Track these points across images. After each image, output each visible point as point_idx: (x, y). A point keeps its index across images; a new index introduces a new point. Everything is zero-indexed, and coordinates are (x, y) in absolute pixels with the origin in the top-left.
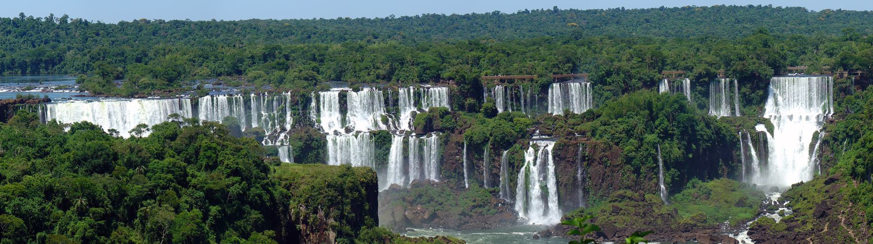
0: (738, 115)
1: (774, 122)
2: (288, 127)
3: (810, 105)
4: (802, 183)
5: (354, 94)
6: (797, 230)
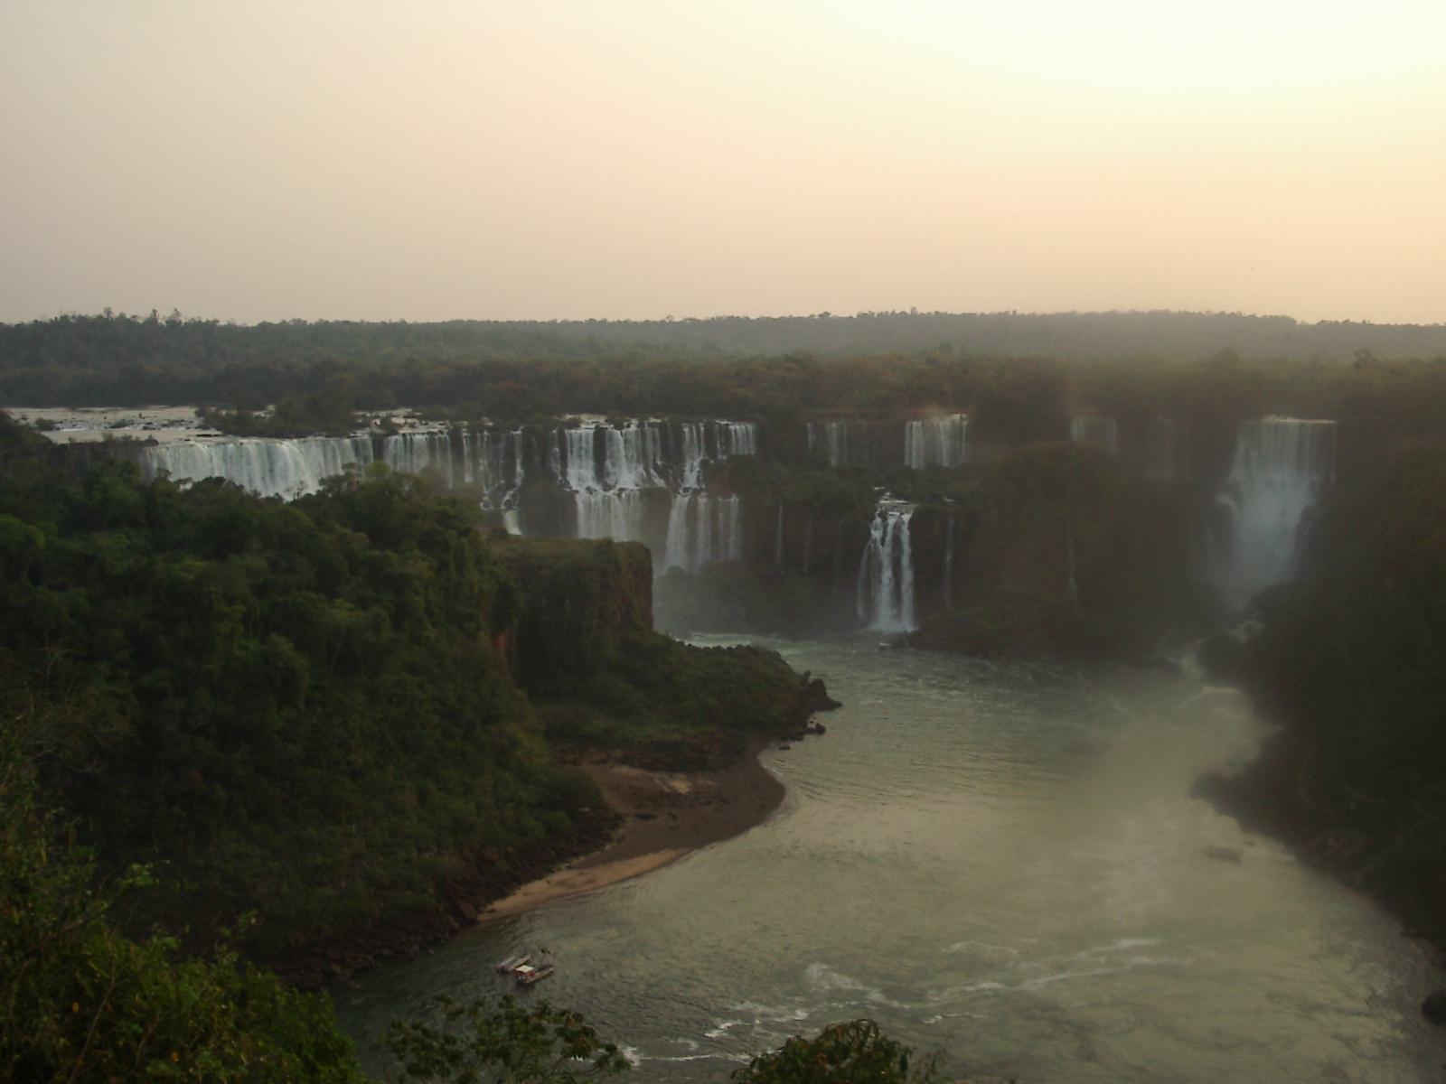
2: (518, 481)
5: (619, 432)
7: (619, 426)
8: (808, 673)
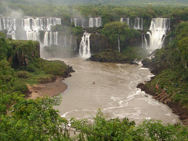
2: (15, 29)
3: (163, 27)
5: (34, 20)
7: (35, 19)
8: (69, 65)
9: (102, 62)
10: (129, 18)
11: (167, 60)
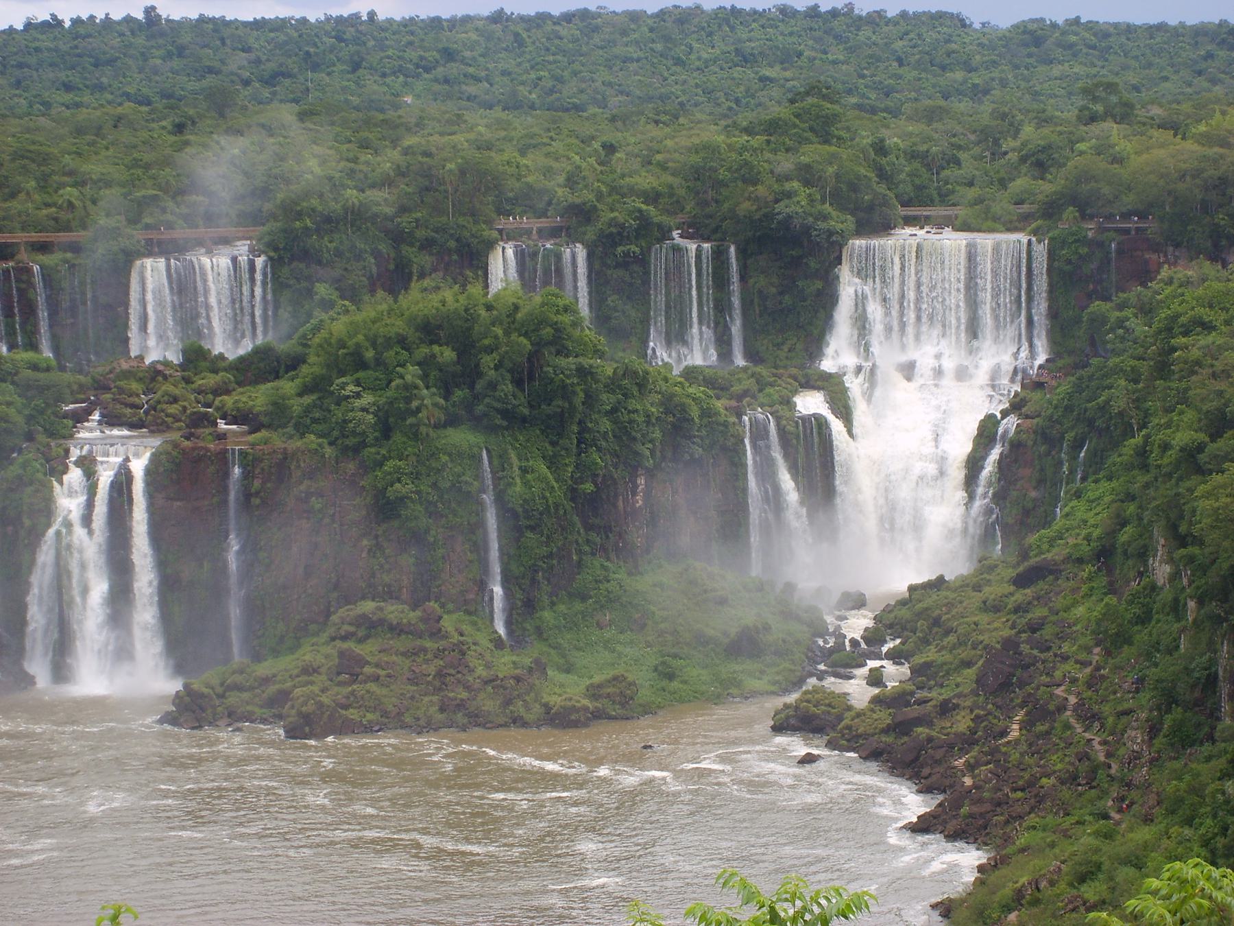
0: (740, 361)
1: (854, 385)
4: (941, 579)
6: (922, 731)
9: (909, 771)
10: (581, 252)
11: (1062, 708)
